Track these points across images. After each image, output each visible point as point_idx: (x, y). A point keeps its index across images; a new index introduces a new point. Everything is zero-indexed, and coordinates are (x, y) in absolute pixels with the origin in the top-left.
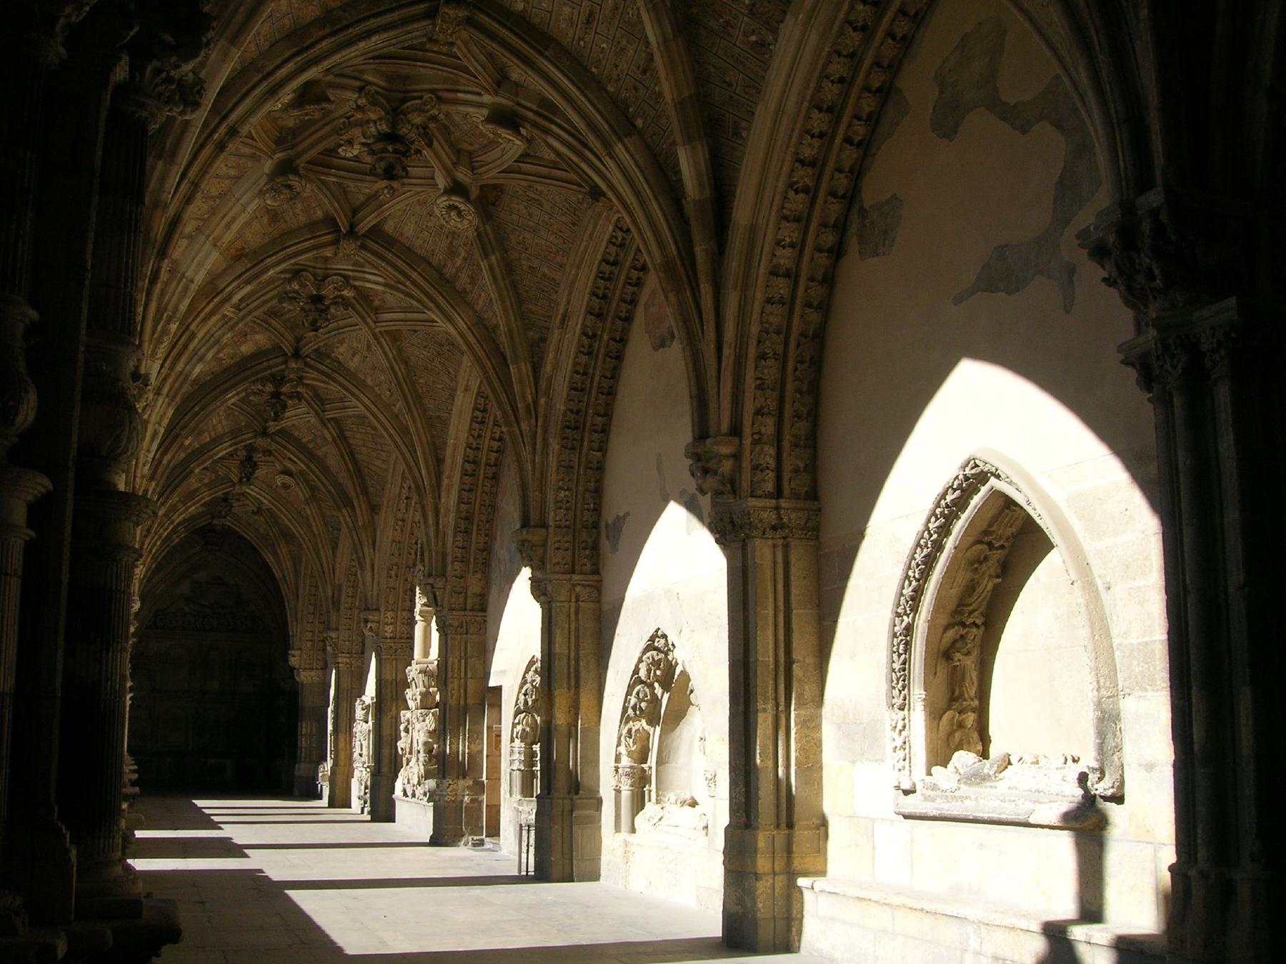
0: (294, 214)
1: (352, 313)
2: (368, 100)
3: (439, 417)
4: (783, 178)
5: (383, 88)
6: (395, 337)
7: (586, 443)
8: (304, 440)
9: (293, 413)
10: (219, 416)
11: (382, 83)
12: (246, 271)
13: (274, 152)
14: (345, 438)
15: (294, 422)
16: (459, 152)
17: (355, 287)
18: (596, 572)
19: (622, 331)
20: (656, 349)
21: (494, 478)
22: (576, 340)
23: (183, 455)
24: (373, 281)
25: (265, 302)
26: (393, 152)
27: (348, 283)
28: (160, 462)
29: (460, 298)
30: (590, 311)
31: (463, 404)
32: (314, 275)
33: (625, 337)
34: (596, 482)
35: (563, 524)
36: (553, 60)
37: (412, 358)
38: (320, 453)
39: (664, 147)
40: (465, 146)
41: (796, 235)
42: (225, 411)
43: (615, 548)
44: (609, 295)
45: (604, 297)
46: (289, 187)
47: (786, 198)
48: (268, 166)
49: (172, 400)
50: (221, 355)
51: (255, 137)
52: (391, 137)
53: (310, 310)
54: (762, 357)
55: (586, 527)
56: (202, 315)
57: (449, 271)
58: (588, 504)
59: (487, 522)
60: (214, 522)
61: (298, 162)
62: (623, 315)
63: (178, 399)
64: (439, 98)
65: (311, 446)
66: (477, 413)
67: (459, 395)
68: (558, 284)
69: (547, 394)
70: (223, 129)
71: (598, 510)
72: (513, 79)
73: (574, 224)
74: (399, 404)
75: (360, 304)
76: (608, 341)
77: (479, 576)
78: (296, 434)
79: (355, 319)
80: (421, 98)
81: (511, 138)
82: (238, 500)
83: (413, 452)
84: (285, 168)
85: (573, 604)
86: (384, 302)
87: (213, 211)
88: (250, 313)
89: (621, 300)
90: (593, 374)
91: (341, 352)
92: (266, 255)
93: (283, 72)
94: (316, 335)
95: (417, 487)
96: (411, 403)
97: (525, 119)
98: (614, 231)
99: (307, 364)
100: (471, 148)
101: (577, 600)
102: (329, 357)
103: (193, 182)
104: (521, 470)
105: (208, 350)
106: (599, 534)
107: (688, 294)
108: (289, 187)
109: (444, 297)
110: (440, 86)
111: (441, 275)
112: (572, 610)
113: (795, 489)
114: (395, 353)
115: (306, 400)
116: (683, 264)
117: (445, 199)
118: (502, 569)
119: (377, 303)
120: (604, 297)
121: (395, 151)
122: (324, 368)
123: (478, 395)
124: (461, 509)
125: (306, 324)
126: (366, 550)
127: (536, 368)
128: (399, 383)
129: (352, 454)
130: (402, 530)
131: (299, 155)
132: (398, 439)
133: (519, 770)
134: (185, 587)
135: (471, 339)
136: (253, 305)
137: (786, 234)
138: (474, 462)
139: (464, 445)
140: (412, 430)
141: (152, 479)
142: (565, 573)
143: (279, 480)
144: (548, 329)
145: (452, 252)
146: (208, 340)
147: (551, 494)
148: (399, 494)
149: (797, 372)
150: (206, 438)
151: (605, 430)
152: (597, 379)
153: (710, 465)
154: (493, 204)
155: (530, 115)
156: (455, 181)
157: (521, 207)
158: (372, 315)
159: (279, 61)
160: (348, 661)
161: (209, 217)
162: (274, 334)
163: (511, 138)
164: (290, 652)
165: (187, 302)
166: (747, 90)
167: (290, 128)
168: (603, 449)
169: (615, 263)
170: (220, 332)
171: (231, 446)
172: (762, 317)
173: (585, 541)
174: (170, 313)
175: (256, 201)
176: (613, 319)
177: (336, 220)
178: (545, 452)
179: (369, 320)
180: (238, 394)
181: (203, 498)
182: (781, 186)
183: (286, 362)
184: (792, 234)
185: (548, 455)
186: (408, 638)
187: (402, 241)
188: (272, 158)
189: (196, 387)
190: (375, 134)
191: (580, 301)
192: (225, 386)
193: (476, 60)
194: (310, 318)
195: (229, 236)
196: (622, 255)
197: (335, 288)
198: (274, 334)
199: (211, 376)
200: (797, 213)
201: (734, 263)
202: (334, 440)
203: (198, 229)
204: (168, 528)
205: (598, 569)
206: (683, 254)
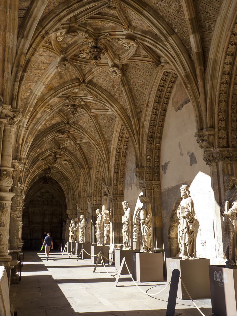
0: (67, 77)
1: (84, 110)
2: (88, 35)
3: (109, 140)
4: (227, 40)
5: (93, 32)
6: (95, 117)
7: (155, 142)
8: (70, 150)
9: (67, 142)
10: (47, 144)
11: (93, 31)
12: (53, 94)
13: (60, 55)
14: (82, 149)
15: (67, 145)
16: (115, 55)
17: (84, 101)
18: (159, 180)
19: (165, 107)
20: (176, 111)
21: (125, 157)
22: (151, 111)
23: (37, 155)
24: (90, 99)
25: (59, 107)
26: (96, 52)
27: (82, 100)
28: (29, 154)
29: (116, 101)
30: (155, 102)
31: (116, 135)
32: (73, 98)
33: (166, 109)
34: (158, 153)
35: (149, 166)
36: (148, 11)
37: (101, 123)
38: (74, 154)
39: (185, 37)
40: (117, 53)
41: (232, 60)
42: (48, 142)
43: (165, 172)
44: (161, 96)
45: (160, 97)
46: (65, 65)
47: (228, 48)
48: (59, 59)
49: (33, 136)
50: (47, 124)
51: (54, 49)
52: (96, 47)
53: (72, 109)
54: (220, 102)
55: (156, 167)
56: (40, 106)
57: (112, 93)
58: (156, 160)
59: (123, 169)
60: (46, 175)
61: (68, 58)
62: (165, 102)
63: (34, 136)
64: (110, 34)
65: (72, 152)
66: (120, 138)
67: (114, 133)
68: (146, 94)
69: (143, 127)
70: (43, 32)
71: (159, 162)
72: (133, 25)
73: (150, 75)
74: (97, 137)
75: (86, 107)
76: (161, 111)
77: (121, 185)
78: (68, 148)
79: (85, 112)
80: (104, 35)
81: (133, 44)
82: (52, 169)
83: (102, 150)
84: (64, 59)
85: (152, 190)
86: (93, 107)
87: (42, 74)
88: (54, 110)
89: (165, 98)
90: (157, 121)
91: (81, 123)
92: (59, 89)
93: (62, 14)
94: (74, 116)
95: (103, 160)
96: (101, 136)
97: (137, 37)
98: (163, 76)
99: (71, 126)
100: (119, 53)
101: (154, 189)
102: (77, 124)
103: (34, 49)
104: (135, 151)
105: (43, 122)
106: (160, 169)
107: (194, 84)
108: (65, 65)
109: (111, 100)
110: (110, 31)
111: (110, 93)
112: (152, 192)
113: (234, 145)
114: (96, 122)
115: (71, 138)
116: (192, 75)
117: (111, 68)
118: (128, 182)
119: (91, 107)
120: (160, 97)
121: (97, 51)
122: (76, 127)
123: (120, 133)
124: (116, 166)
125: (71, 112)
127: (139, 120)
128: (97, 130)
129: (84, 153)
130: (98, 174)
131: (68, 56)
132: (97, 146)
133: (135, 241)
134: (38, 194)
135: (120, 113)
136: (55, 108)
137: (228, 60)
138: (119, 152)
139: (116, 147)
140: (101, 144)
141: (27, 159)
142: (150, 181)
143: (64, 162)
144: (143, 108)
145: (113, 87)
146: (43, 119)
147: (145, 157)
148: (97, 164)
149: (233, 106)
150: (43, 150)
151: (161, 138)
152: (158, 122)
153: (204, 138)
154: (126, 71)
155: (139, 36)
156: (114, 63)
157: (134, 71)
158: (89, 111)
159: (61, 10)
160: (83, 212)
161: (41, 76)
162: (61, 117)
163: (133, 44)
164: (67, 210)
165: (35, 101)
166: (213, 13)
167: (65, 47)
168: (160, 143)
169: (163, 86)
170: (46, 116)
171: (50, 152)
172: (220, 89)
173: (156, 171)
174: (30, 105)
175: (56, 70)
176: (162, 104)
177: (79, 79)
178: (143, 145)
179: (88, 112)
180: (52, 137)
181: (43, 168)
182: (227, 44)
183: (65, 126)
184: (230, 60)
185: (143, 146)
186: (100, 205)
187: (98, 84)
188: (60, 57)
189: (40, 133)
190: (91, 46)
191: (152, 99)
192: (47, 133)
193: (122, 17)
194: (72, 111)
195: (47, 82)
196: (165, 84)
197: (79, 102)
198: (61, 117)
199: (44, 130)
200: (232, 53)
201: (209, 72)
202: (79, 149)
203: (38, 80)
204: (33, 176)
205: (160, 179)
206: (192, 71)
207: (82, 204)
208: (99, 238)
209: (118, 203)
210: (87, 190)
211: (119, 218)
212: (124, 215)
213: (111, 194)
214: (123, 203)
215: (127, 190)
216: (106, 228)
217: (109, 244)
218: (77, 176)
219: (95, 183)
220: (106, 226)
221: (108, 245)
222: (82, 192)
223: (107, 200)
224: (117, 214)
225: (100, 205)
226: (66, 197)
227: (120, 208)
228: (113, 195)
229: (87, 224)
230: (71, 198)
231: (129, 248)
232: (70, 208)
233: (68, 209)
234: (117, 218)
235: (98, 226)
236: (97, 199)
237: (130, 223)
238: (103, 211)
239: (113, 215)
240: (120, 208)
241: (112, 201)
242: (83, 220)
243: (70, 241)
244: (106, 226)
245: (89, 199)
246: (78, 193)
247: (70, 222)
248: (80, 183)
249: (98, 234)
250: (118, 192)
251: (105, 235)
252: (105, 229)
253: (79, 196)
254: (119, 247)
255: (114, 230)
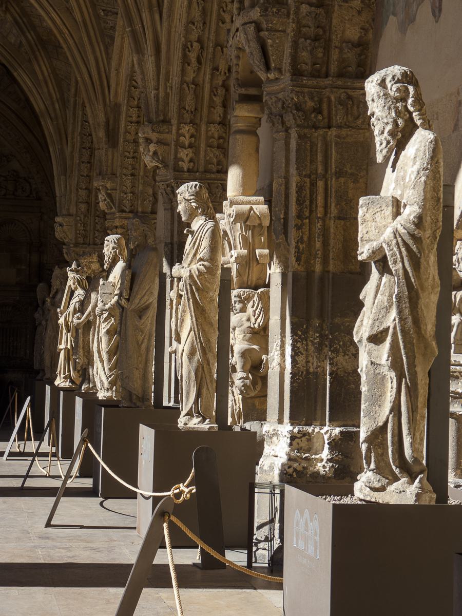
126: (145, 15)
164: (58, 219)
186: (218, 172)
207: (128, 180)
208: (193, 374)
209: (333, 132)
210: (143, 79)
211: (332, 242)
212: (373, 188)
213: (280, 70)
214: (371, 86)
215: (403, 28)
216: (243, 310)
217: (262, 417)
218: (98, 16)
219: (187, 31)
220: (248, 299)
221: (252, 426)
222: (124, 108)
223: (259, 131)
224: (320, 212)
225: (219, 176)
226: (51, 149)
227: (339, 174)
228: (297, 73)
229: (131, 289)
230: (76, 155)
231: (412, 481)
232: (73, 210)
233: (63, 215)
234: (318, 245)
235: (184, 300)
236: (203, 137)
237: (433, 258)
238: (232, 203)
239: (292, 222)
240: (339, 174)
241: (289, 119)
242: (120, 265)
243: (59, 382)
244: (244, 301)
245: (154, 136)
246: (102, 118)
247: (66, 278)
248: (115, 57)
249: (187, 349)
250: (335, 55)
251: (235, 359)
252: (234, 319)
253: (108, 136)
254: (327, 446)
255: (292, 324)
